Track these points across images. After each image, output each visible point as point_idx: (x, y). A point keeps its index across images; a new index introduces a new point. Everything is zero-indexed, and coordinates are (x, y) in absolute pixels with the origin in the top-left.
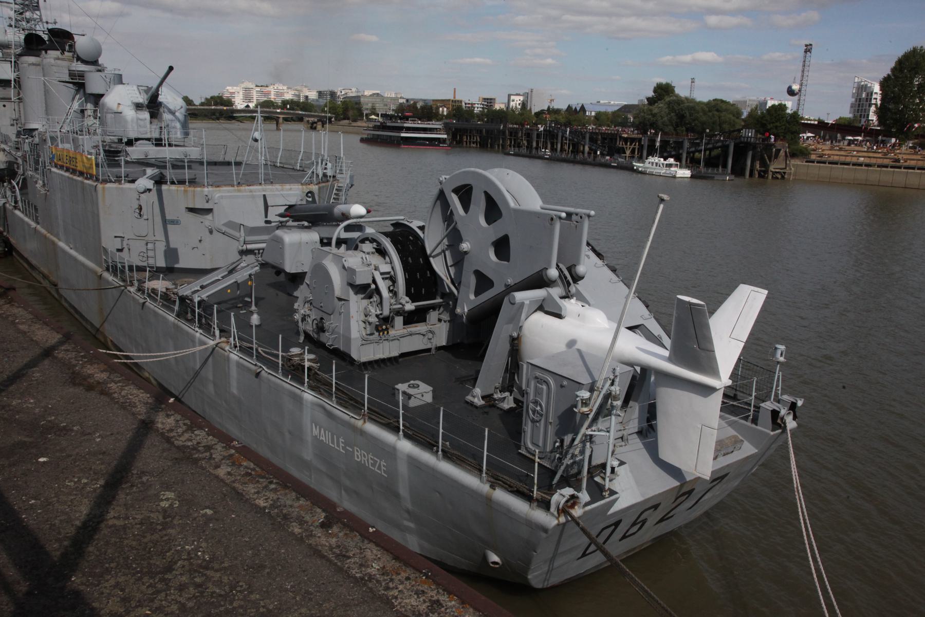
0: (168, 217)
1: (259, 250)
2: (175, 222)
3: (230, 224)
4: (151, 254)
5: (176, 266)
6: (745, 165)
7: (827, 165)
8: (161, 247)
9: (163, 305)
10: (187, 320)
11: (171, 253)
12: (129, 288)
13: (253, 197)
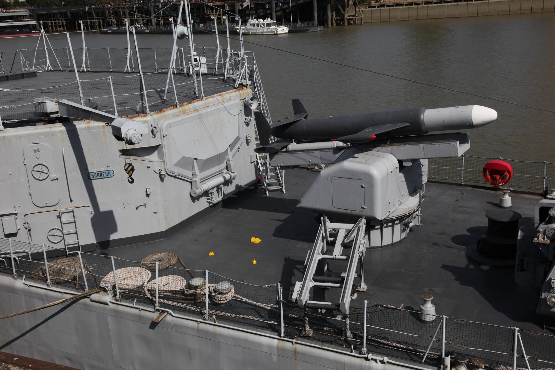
0: (91, 169)
1: (213, 188)
2: (100, 175)
3: (185, 162)
4: (69, 229)
5: (113, 237)
6: (327, 17)
7: (386, 8)
8: (86, 215)
9: (219, 318)
10: (348, 344)
11: (104, 221)
12: (95, 296)
13: (200, 117)
